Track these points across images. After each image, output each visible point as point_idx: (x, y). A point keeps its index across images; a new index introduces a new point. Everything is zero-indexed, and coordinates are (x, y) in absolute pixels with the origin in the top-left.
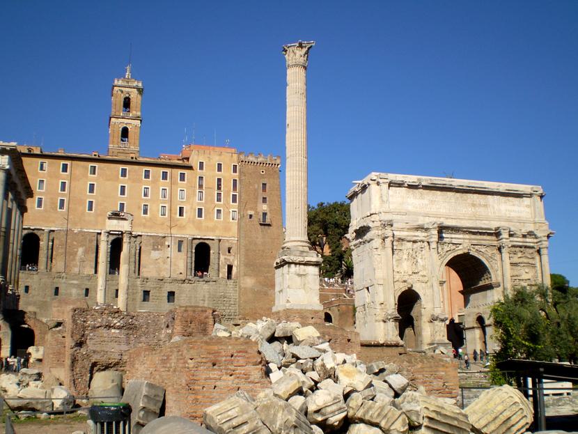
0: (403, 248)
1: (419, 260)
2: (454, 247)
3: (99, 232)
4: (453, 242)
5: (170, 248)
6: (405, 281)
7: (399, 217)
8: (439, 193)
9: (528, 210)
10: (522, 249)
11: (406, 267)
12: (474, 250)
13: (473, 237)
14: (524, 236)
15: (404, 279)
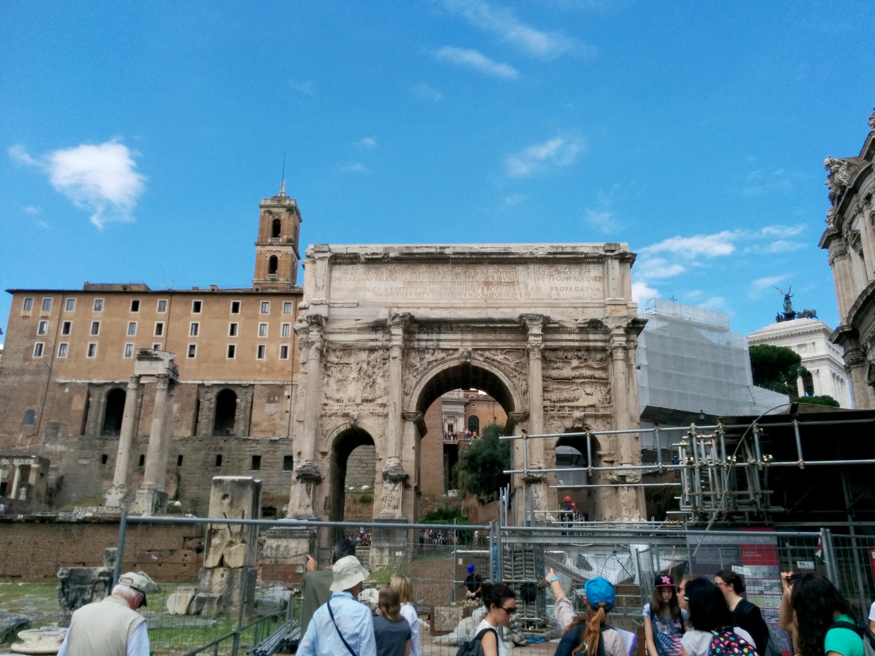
0: (352, 360)
1: (379, 380)
2: (444, 355)
3: (201, 382)
4: (441, 347)
5: (289, 400)
6: (346, 415)
7: (344, 311)
8: (423, 268)
9: (598, 285)
10: (580, 354)
11: (353, 390)
12: (482, 359)
13: (480, 336)
14: (582, 330)
15: (347, 411)
